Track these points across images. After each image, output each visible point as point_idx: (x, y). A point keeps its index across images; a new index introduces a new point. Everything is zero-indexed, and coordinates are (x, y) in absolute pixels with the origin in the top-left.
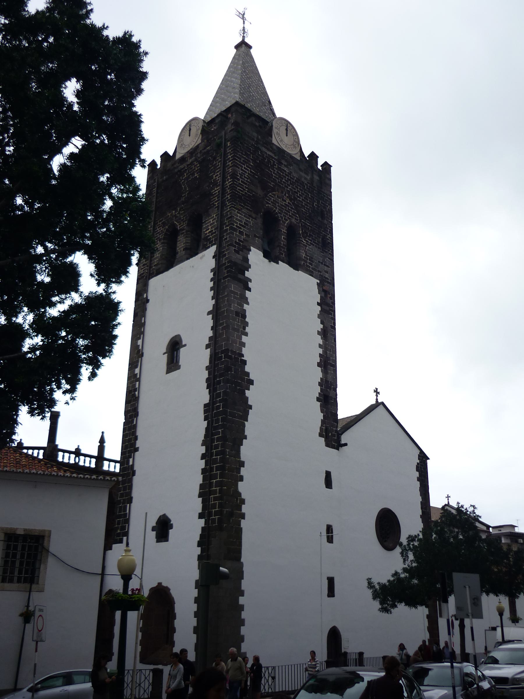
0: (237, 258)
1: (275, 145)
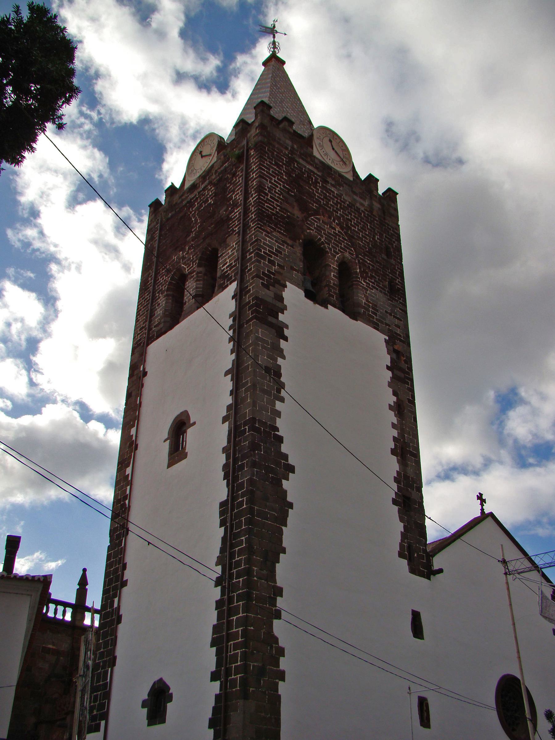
0: (267, 295)
1: (317, 159)
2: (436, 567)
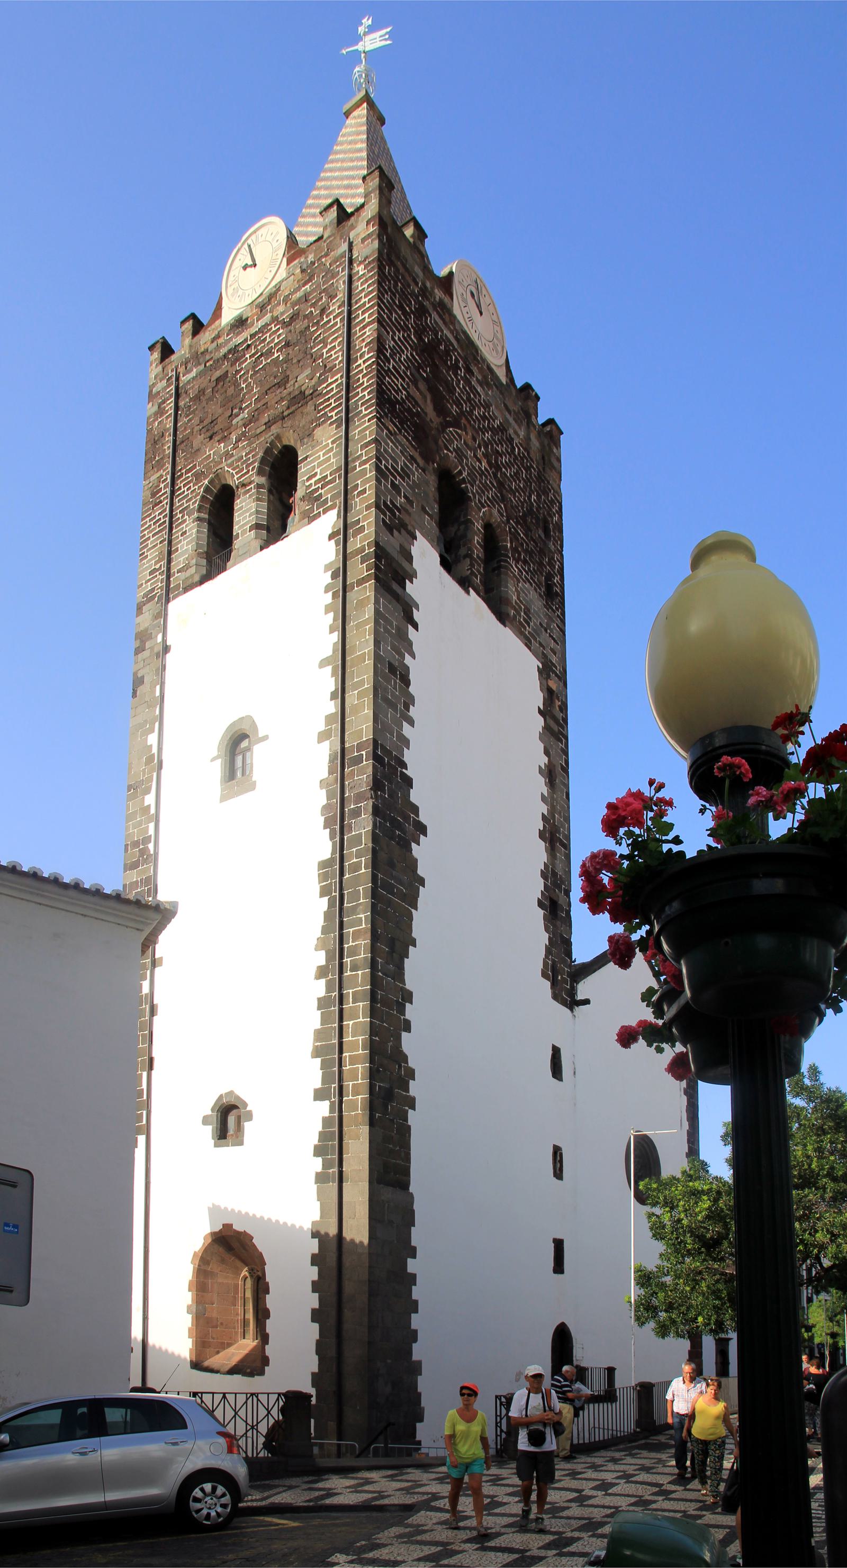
0: (392, 542)
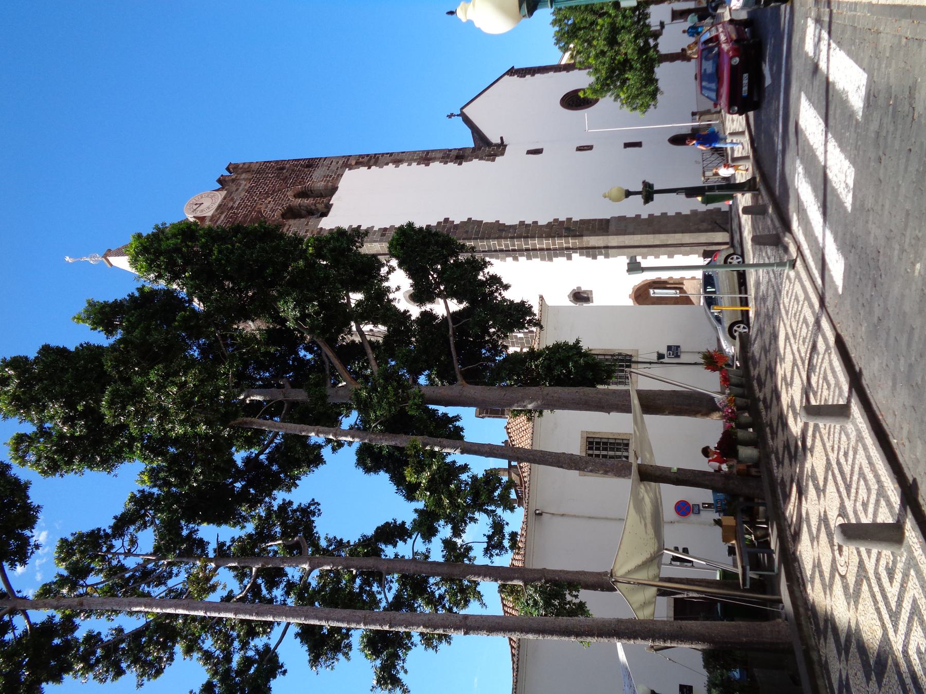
2: (499, 142)
